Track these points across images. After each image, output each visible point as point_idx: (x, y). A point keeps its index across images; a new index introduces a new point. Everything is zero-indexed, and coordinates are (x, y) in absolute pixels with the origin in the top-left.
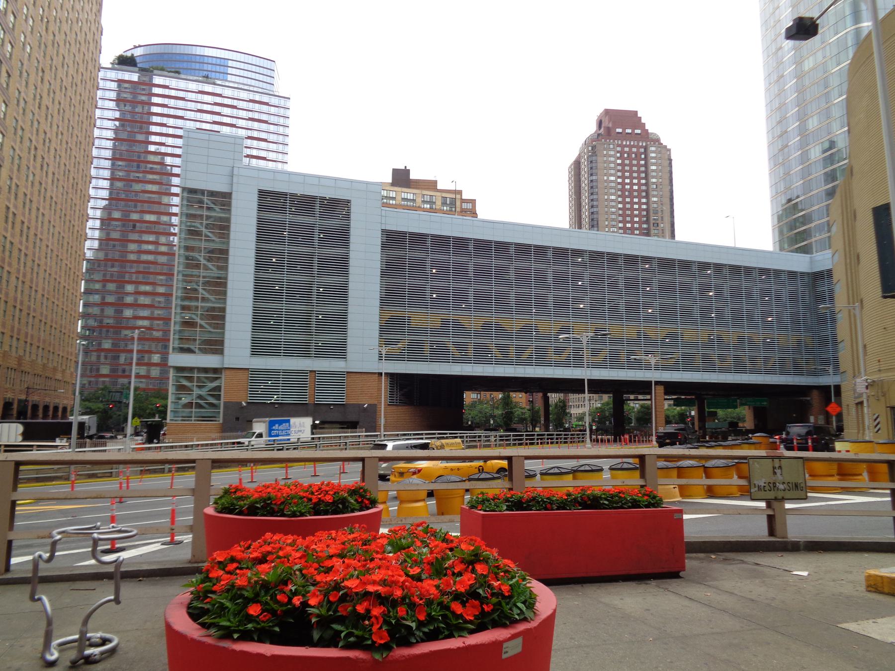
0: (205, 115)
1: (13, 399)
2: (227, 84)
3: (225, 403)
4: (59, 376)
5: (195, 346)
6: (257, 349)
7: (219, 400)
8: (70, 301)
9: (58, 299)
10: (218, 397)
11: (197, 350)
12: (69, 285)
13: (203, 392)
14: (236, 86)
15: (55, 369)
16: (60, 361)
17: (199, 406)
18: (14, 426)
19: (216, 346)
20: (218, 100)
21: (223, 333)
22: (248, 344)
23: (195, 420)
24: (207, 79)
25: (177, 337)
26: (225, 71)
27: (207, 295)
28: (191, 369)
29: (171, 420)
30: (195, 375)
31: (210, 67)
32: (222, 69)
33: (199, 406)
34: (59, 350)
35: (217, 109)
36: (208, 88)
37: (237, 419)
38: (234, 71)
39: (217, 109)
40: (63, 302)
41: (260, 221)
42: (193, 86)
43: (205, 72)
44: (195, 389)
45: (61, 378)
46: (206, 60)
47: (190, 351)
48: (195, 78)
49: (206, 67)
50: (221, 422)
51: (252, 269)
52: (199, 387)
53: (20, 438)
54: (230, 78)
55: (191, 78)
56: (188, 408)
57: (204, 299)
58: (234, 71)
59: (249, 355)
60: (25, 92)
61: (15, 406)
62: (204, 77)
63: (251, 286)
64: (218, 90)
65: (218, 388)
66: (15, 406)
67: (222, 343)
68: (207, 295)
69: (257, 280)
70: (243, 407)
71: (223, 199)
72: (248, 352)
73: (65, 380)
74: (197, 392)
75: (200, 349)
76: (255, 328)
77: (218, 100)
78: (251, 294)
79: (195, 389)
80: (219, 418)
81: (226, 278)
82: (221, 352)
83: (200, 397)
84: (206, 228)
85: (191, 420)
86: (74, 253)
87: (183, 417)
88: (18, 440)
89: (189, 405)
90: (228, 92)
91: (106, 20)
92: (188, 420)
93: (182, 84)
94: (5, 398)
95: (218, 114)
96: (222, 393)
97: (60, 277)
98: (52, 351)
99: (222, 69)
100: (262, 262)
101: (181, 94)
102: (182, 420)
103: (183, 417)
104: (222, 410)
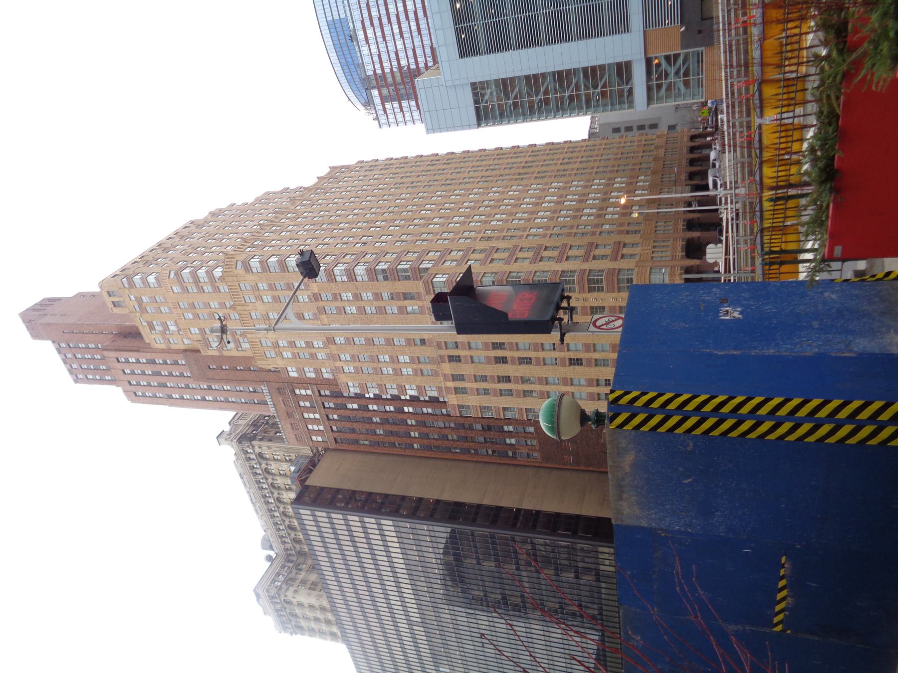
0: (386, 33)
2: (349, 17)
3: (682, 48)
4: (661, 152)
6: (621, 25)
7: (679, 55)
8: (592, 153)
9: (593, 168)
10: (676, 56)
11: (629, 86)
12: (577, 158)
13: (672, 71)
14: (347, 8)
15: (656, 159)
16: (648, 153)
17: (686, 74)
18: (708, 251)
19: (623, 70)
20: (367, 23)
21: (609, 65)
22: (617, 37)
23: (702, 74)
24: (353, 38)
26: (339, 21)
28: (649, 89)
29: (702, 98)
30: (655, 83)
31: (342, 37)
32: (338, 25)
33: (686, 74)
34: (637, 157)
35: (376, 22)
36: (361, 35)
37: (700, 32)
38: (335, 13)
39: (376, 22)
40: (595, 161)
41: (490, 51)
42: (365, 50)
43: (348, 41)
44: (668, 81)
45: (663, 150)
46: (337, 42)
47: (630, 92)
48: (357, 48)
49: (343, 41)
51: (538, 49)
52: (667, 75)
53: (719, 245)
54: (343, 16)
55: (357, 50)
56: (689, 83)
58: (335, 13)
59: (629, 34)
60: (436, 235)
62: (352, 41)
63: (556, 47)
64: (359, 25)
65: (667, 58)
67: (619, 65)
69: (549, 42)
70: (687, 29)
71: (478, 89)
72: (625, 36)
73: (664, 144)
74: (672, 78)
75: (627, 84)
77: (367, 23)
78: (565, 45)
79: (668, 81)
80: (698, 51)
81: (554, 73)
82: (628, 64)
83: (677, 73)
84: (509, 99)
85: (702, 78)
86: (549, 157)
87: (699, 86)
88: (721, 248)
89: (686, 84)
90: (357, 15)
91: (351, 161)
92: (702, 81)
93: (367, 60)
95: (380, 19)
96: (672, 53)
97: (572, 169)
98: (639, 167)
99: (338, 25)
100: (529, 40)
101: (376, 59)
102: (702, 86)
103: (699, 86)
104: (691, 50)
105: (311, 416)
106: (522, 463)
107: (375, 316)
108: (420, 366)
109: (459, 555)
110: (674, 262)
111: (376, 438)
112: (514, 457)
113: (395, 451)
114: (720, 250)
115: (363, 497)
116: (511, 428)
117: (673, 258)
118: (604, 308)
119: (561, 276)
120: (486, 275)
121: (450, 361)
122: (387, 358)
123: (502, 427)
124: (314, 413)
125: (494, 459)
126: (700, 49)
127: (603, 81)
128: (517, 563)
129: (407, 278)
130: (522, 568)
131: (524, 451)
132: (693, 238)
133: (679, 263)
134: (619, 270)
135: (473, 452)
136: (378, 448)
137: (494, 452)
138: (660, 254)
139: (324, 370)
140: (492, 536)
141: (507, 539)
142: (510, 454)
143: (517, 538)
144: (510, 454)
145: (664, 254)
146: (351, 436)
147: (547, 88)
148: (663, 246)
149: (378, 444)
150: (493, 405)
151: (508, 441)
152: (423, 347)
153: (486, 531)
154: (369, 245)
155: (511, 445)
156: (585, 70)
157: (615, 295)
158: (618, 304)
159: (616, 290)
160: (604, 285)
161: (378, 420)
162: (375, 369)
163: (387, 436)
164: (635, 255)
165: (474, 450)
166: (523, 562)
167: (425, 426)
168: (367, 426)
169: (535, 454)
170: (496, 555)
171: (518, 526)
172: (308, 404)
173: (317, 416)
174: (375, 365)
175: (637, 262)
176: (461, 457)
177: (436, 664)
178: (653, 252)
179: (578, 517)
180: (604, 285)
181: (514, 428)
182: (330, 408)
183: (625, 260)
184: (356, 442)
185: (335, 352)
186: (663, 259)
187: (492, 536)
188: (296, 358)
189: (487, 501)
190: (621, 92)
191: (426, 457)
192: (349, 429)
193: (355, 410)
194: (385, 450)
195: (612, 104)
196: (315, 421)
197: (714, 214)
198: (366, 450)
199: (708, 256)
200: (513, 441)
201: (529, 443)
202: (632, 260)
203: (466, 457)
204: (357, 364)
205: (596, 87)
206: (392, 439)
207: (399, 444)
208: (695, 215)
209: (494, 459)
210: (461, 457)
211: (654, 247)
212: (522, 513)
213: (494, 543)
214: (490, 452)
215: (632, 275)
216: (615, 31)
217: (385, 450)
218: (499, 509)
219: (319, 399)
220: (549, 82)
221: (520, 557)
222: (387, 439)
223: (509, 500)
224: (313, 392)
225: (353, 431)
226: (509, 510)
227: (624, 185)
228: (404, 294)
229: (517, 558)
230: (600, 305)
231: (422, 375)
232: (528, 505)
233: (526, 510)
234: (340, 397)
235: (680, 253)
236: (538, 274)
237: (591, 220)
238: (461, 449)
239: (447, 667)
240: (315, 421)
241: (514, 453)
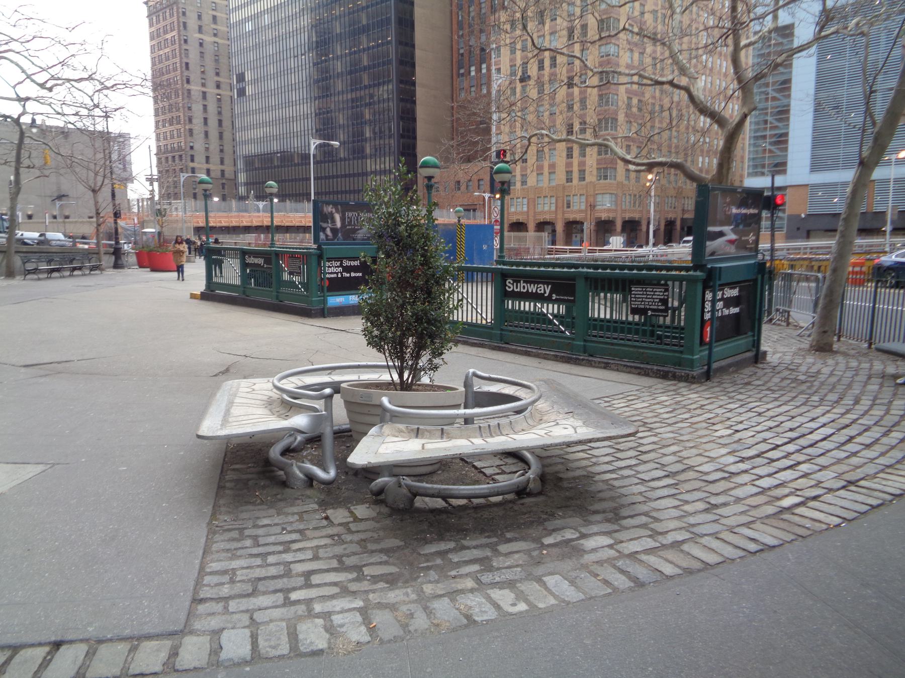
1: (675, 219)
5: (766, 170)
11: (766, 172)
19: (780, 167)
21: (786, 156)
22: (807, 162)
25: (751, 163)
27: (777, 124)
37: (798, 229)
50: (785, 232)
53: (622, 246)
57: (776, 127)
61: (678, 223)
66: (678, 223)
68: (777, 124)
72: (808, 169)
76: (814, 147)
94: (667, 218)
104: (786, 222)
106: (454, 83)
109: (369, 30)
110: (619, 212)
112: (459, 75)
114: (618, 246)
116: (484, 71)
117: (624, 211)
118: (585, 156)
119: (612, 119)
120: (616, 47)
123: (485, 63)
125: (455, 55)
126: (785, 229)
127: (775, 150)
128: (370, 86)
130: (367, 91)
131: (465, 84)
132: (641, 225)
133: (619, 216)
134: (615, 169)
135: (461, 34)
137: (462, 55)
138: (628, 200)
140: (389, 62)
141: (389, 76)
142: (462, 71)
143: (390, 87)
144: (462, 71)
145: (628, 204)
147: (779, 100)
148: (635, 203)
150: (502, 58)
151: (473, 68)
153: (393, 56)
155: (470, 72)
156: (786, 134)
157: (595, 166)
158: (587, 168)
159: (599, 166)
160: (603, 156)
164: (629, 180)
165: (463, 34)
166: (371, 91)
169: (463, 95)
170: (374, 66)
171: (401, 86)
175: (622, 182)
176: (455, 22)
177: (269, 11)
178: (631, 195)
179: (415, 138)
180: (603, 156)
181: (484, 74)
183: (624, 173)
186: (623, 203)
187: (389, 62)
189: (418, 53)
190: (763, 166)
195: (754, 159)
197: (643, 241)
199: (615, 238)
200: (473, 74)
201: (473, 89)
202: (624, 178)
203: (455, 26)
205: (771, 144)
208: (644, 228)
209: (455, 55)
210: (455, 22)
211: (635, 196)
212: (412, 88)
213: (384, 64)
214: (462, 51)
215: (610, 179)
216: (814, 157)
218: (413, 65)
220: (785, 101)
221: (376, 89)
223: (421, 75)
226: (413, 74)
227: (700, 165)
229: (374, 85)
230: (587, 153)
232: (420, 93)
233: (414, 91)
235: (627, 216)
236: (616, 97)
237: (699, 123)
238: (462, 21)
239: (270, 22)
241: (463, 75)
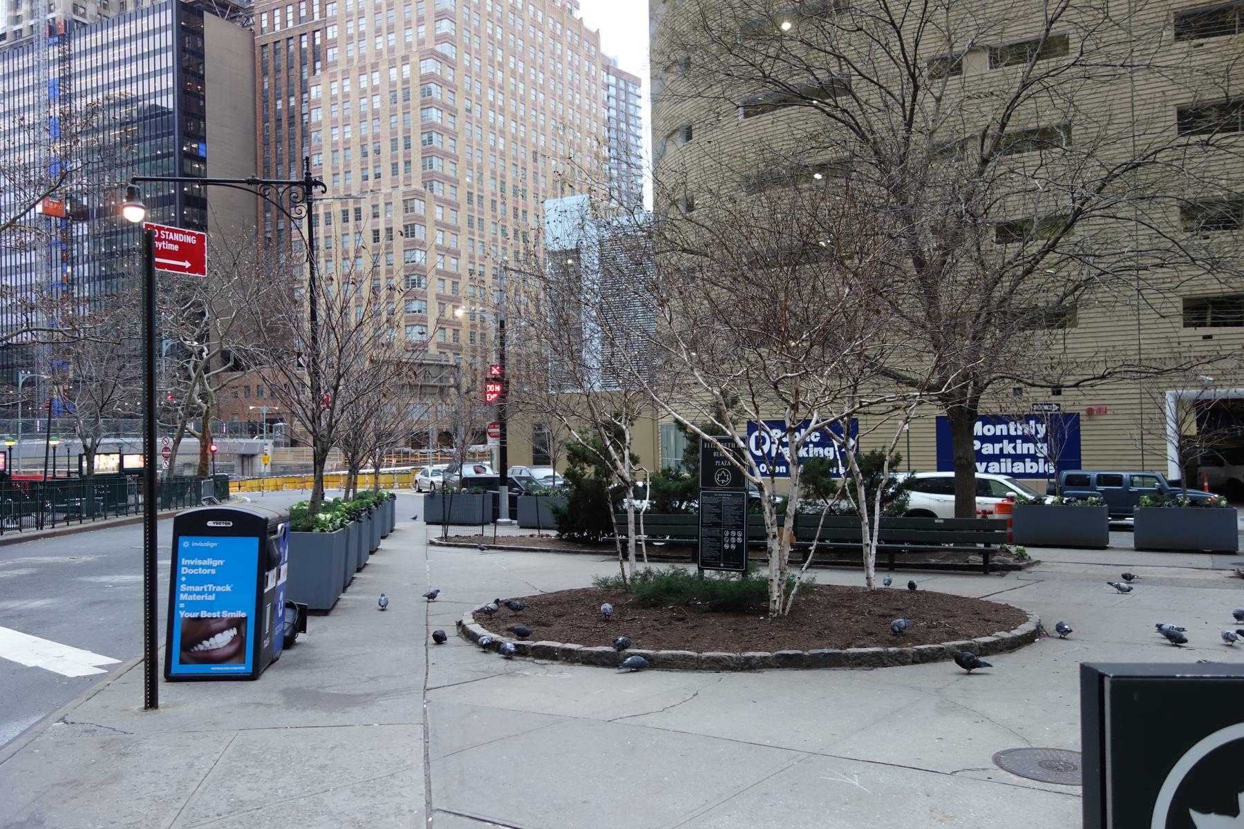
105: (290, 17)
107: (388, 127)
108: (342, 173)
111: (271, 100)
113: (259, 122)
115: (194, 111)
121: (343, 211)
122: (348, 136)
124: (294, 20)
129: (424, 167)
136: (262, 100)
139: (336, 50)
146: (271, 67)
149: (265, 101)
152: (360, 178)
154: (467, 116)
161: (292, 104)
162: (336, 120)
163: (275, 113)
167: (290, 162)
168: (284, 89)
172: (303, 13)
173: (290, 24)
174: (340, 121)
182: (301, 43)
184: (265, 74)
185: (351, 75)
188: (347, 16)
191: (256, 158)
192: (279, 65)
193: (301, 76)
194: (259, 110)
196: (284, 22)
198: (258, 86)
204: (340, 99)
206: (272, 119)
207: (268, 127)
214: (269, 235)
217: (259, 110)
219: (310, 30)
222: (271, 113)
224: (317, 23)
225: (277, 71)
228: (410, 162)
231: (334, 175)
234: (314, 58)
240: (284, 22)
